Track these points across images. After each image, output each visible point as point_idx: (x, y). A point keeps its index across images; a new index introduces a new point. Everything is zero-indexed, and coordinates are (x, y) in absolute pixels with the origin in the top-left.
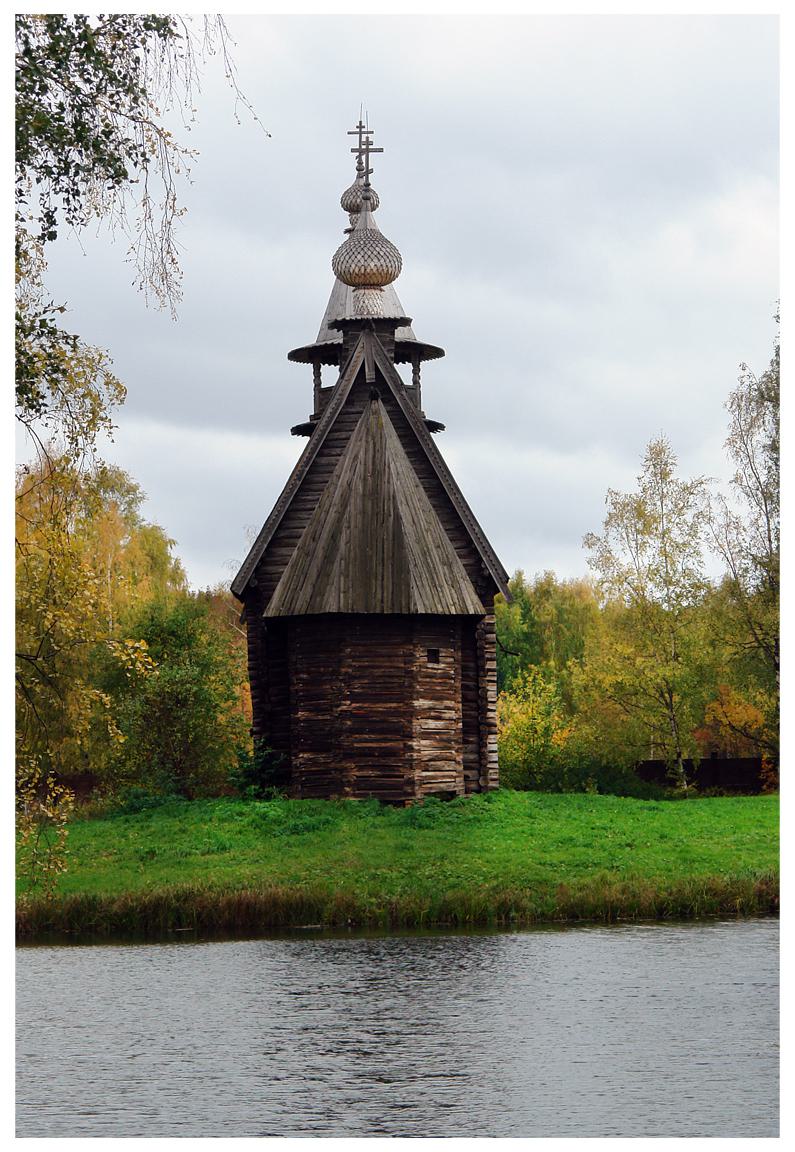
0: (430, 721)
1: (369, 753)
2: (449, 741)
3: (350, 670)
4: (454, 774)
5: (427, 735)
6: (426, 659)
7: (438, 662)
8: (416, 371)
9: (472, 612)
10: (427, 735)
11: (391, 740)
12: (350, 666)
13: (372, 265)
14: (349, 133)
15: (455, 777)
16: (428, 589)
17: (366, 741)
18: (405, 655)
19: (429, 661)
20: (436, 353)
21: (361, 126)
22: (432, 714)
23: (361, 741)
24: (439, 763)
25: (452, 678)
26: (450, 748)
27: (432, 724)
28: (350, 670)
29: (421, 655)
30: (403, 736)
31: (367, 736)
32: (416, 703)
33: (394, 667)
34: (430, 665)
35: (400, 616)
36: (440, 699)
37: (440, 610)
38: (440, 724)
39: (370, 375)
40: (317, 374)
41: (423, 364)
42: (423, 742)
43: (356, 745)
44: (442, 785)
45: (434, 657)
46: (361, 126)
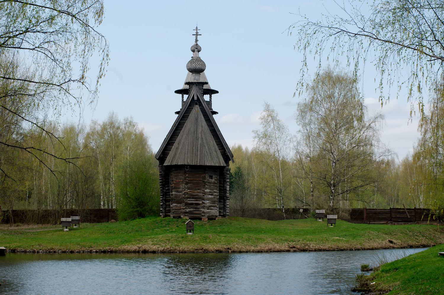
1: (192, 204)
2: (215, 201)
3: (187, 181)
4: (216, 210)
5: (208, 199)
7: (212, 179)
8: (211, 97)
9: (222, 165)
10: (208, 199)
12: (187, 180)
18: (203, 177)
20: (217, 92)
21: (197, 28)
22: (210, 194)
26: (215, 203)
27: (210, 196)
28: (187, 181)
29: (207, 176)
34: (210, 180)
36: (213, 190)
38: (212, 196)
39: (196, 98)
40: (183, 97)
41: (213, 95)
42: (208, 202)
43: (189, 202)
45: (211, 177)
46: (197, 28)
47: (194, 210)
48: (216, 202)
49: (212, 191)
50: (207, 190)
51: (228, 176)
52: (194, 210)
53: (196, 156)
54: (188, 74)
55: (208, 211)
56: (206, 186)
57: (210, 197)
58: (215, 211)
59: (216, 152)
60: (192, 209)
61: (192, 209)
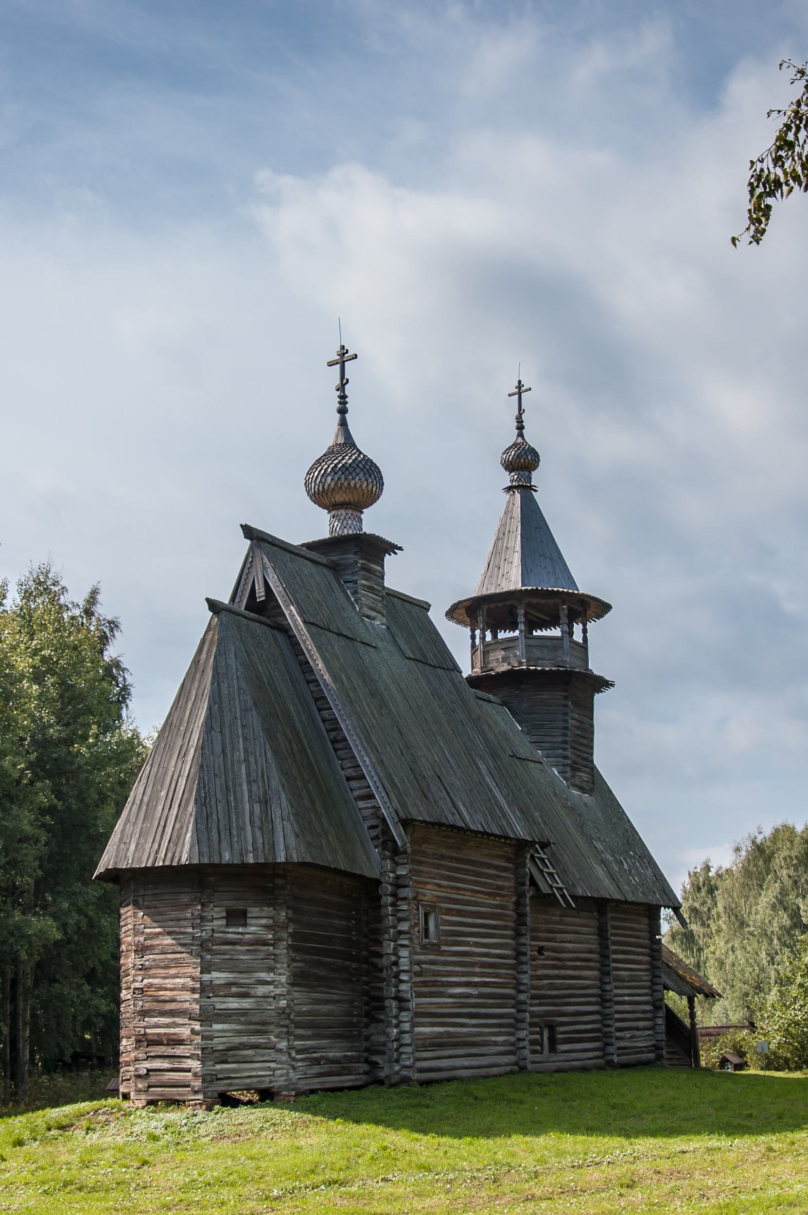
0: (231, 999)
4: (273, 1065)
6: (224, 922)
7: (245, 925)
8: (585, 625)
9: (281, 858)
14: (510, 395)
15: (274, 1070)
16: (215, 837)
17: (157, 1026)
19: (227, 926)
21: (520, 385)
22: (234, 989)
25: (270, 945)
26: (265, 1032)
27: (233, 1004)
30: (190, 1019)
31: (156, 1019)
33: (182, 933)
35: (211, 865)
37: (227, 857)
38: (246, 1003)
40: (473, 637)
44: (248, 1081)
45: (236, 917)
48: (272, 1028)
49: (243, 979)
50: (215, 974)
51: (405, 907)
53: (161, 828)
57: (235, 1006)
58: (269, 1068)
59: (265, 803)
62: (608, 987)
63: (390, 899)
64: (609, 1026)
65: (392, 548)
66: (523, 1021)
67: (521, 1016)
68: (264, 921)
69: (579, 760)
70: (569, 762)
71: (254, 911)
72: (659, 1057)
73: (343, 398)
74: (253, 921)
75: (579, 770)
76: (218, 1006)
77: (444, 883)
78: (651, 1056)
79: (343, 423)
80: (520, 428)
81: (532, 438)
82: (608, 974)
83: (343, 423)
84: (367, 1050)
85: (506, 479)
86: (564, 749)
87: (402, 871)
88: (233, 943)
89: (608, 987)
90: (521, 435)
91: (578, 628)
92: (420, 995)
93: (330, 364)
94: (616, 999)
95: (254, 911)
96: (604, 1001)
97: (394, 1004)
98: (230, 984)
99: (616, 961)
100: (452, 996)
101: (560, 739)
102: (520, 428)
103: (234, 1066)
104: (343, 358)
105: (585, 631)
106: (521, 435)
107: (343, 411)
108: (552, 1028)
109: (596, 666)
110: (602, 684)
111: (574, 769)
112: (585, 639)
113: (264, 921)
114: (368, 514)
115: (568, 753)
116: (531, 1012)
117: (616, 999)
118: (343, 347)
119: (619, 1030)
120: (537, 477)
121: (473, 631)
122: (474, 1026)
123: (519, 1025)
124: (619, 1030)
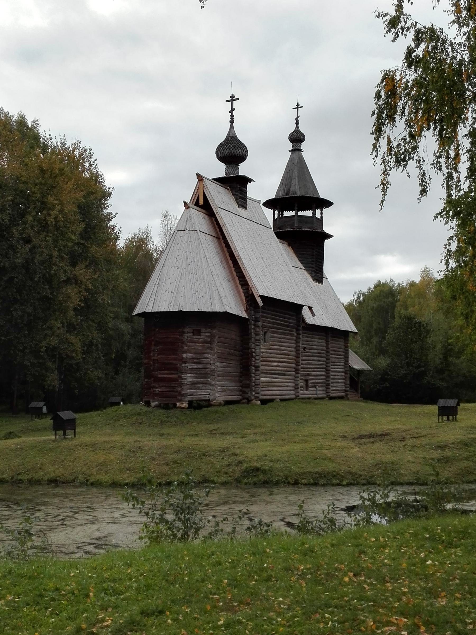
0: (194, 364)
4: (209, 391)
5: (192, 370)
6: (192, 334)
7: (200, 335)
8: (322, 211)
10: (192, 370)
11: (173, 374)
13: (227, 152)
19: (193, 335)
20: (326, 204)
23: (161, 374)
24: (199, 385)
26: (206, 378)
27: (195, 366)
32: (184, 355)
34: (194, 337)
38: (200, 366)
40: (274, 214)
42: (189, 375)
44: (200, 396)
47: (167, 389)
49: (198, 356)
52: (167, 389)
54: (225, 167)
55: (190, 392)
56: (186, 348)
57: (196, 367)
60: (164, 389)
61: (164, 389)
62: (328, 365)
63: (253, 327)
64: (329, 381)
65: (250, 180)
66: (298, 377)
67: (297, 375)
68: (207, 334)
69: (318, 269)
70: (314, 269)
71: (203, 330)
72: (347, 395)
73: (232, 116)
74: (203, 334)
75: (317, 273)
76: (189, 367)
77: (272, 320)
78: (344, 394)
79: (232, 127)
80: (297, 123)
81: (301, 128)
82: (328, 359)
83: (232, 127)
84: (241, 386)
85: (290, 146)
86: (312, 264)
87: (258, 315)
88: (195, 342)
89: (328, 365)
90: (297, 127)
91: (318, 211)
92: (262, 365)
93: (227, 101)
94: (332, 370)
95: (203, 330)
96: (327, 371)
97: (253, 368)
98: (194, 358)
99: (332, 354)
100: (273, 366)
101: (310, 260)
102: (297, 123)
103: (195, 390)
104: (233, 99)
105: (322, 214)
106: (297, 127)
107: (232, 122)
108: (307, 381)
109: (326, 229)
110: (328, 236)
111: (316, 273)
112: (322, 217)
113: (207, 334)
114: (241, 166)
115: (314, 266)
116: (301, 374)
117: (332, 370)
118: (233, 94)
119: (332, 383)
120: (304, 146)
121: (274, 212)
122: (281, 379)
123: (296, 379)
124: (332, 383)
